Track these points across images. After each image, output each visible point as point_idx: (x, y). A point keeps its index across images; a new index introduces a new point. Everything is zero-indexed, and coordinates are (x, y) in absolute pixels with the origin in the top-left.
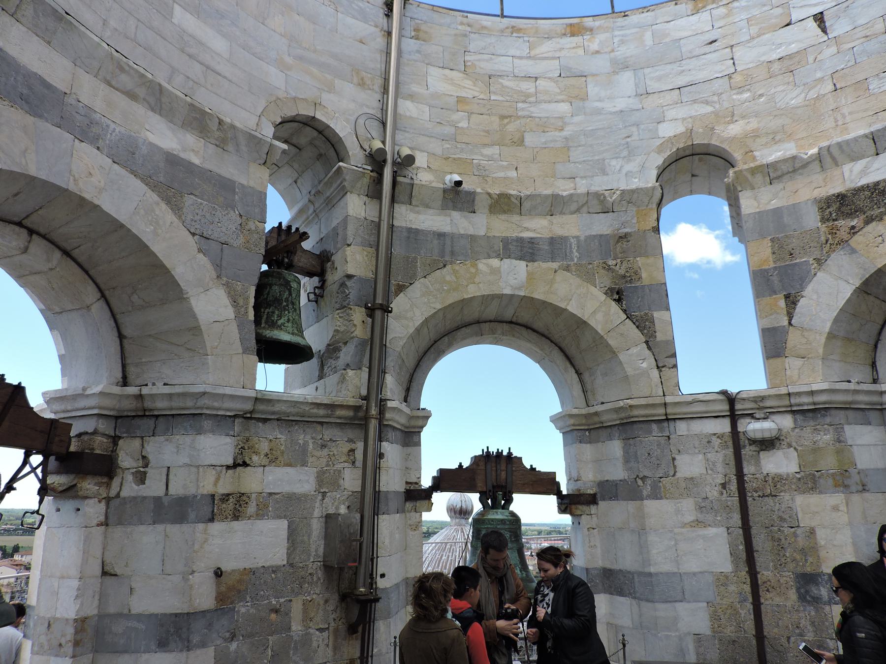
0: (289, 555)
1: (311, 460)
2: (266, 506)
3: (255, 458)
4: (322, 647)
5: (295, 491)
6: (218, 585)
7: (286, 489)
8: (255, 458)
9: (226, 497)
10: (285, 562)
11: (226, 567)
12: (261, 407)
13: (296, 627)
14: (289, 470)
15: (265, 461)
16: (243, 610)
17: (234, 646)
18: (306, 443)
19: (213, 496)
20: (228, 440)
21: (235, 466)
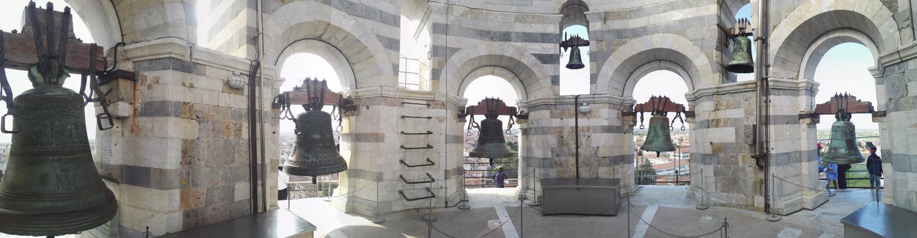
0: (736, 139)
1: (742, 106)
2: (727, 123)
3: (721, 107)
4: (750, 173)
5: (737, 117)
6: (713, 147)
7: (734, 116)
8: (721, 107)
9: (713, 120)
10: (735, 141)
11: (713, 142)
12: (720, 90)
13: (740, 164)
14: (734, 110)
15: (726, 108)
16: (721, 155)
17: (719, 166)
18: (740, 100)
19: (708, 120)
20: (712, 102)
21: (715, 110)
